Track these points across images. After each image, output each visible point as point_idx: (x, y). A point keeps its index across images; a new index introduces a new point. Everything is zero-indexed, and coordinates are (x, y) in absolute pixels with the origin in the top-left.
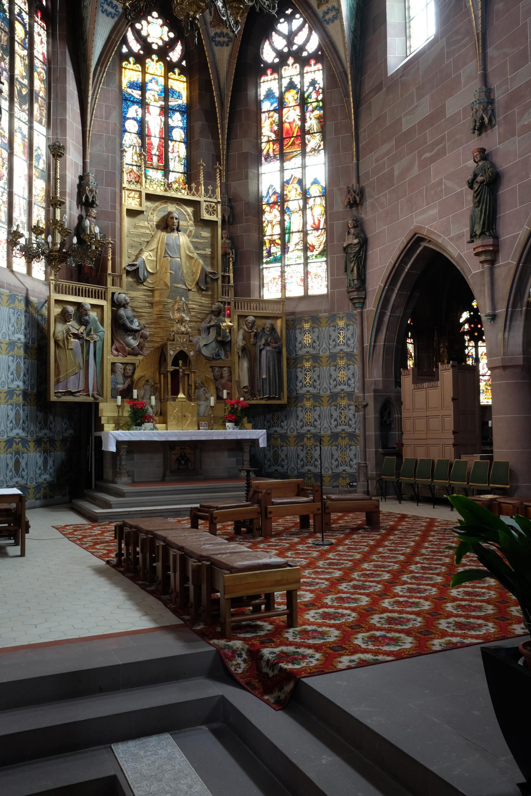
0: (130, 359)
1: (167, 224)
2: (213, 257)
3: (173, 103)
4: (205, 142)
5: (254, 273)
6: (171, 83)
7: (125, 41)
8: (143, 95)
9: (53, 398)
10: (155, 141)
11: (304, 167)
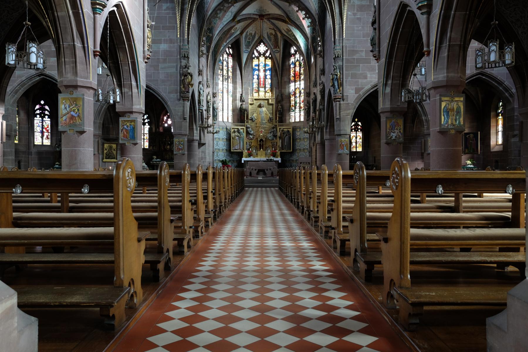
1: (260, 106)
2: (273, 113)
3: (267, 68)
4: (274, 79)
5: (287, 115)
6: (267, 62)
7: (253, 53)
10: (262, 80)
11: (300, 84)
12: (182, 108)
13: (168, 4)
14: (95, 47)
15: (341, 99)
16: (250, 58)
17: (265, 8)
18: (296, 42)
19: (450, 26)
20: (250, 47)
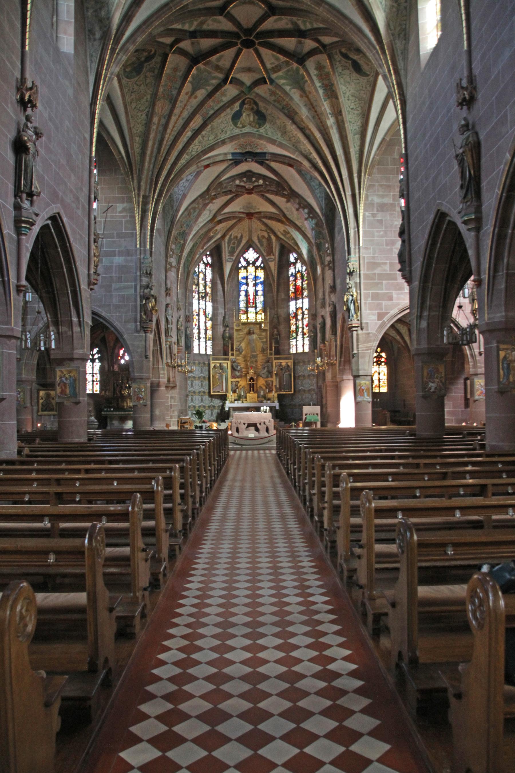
0: (237, 379)
1: (249, 333)
2: (266, 342)
3: (257, 282)
7: (240, 262)
8: (247, 281)
9: (212, 393)
10: (251, 297)
11: (303, 303)
12: (143, 343)
13: (125, 205)
14: (18, 279)
15: (359, 328)
16: (236, 269)
17: (254, 205)
18: (296, 248)
19: (507, 249)
20: (235, 254)
